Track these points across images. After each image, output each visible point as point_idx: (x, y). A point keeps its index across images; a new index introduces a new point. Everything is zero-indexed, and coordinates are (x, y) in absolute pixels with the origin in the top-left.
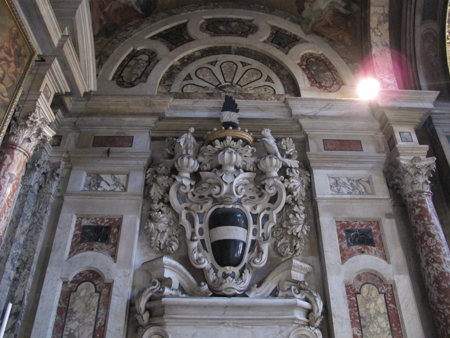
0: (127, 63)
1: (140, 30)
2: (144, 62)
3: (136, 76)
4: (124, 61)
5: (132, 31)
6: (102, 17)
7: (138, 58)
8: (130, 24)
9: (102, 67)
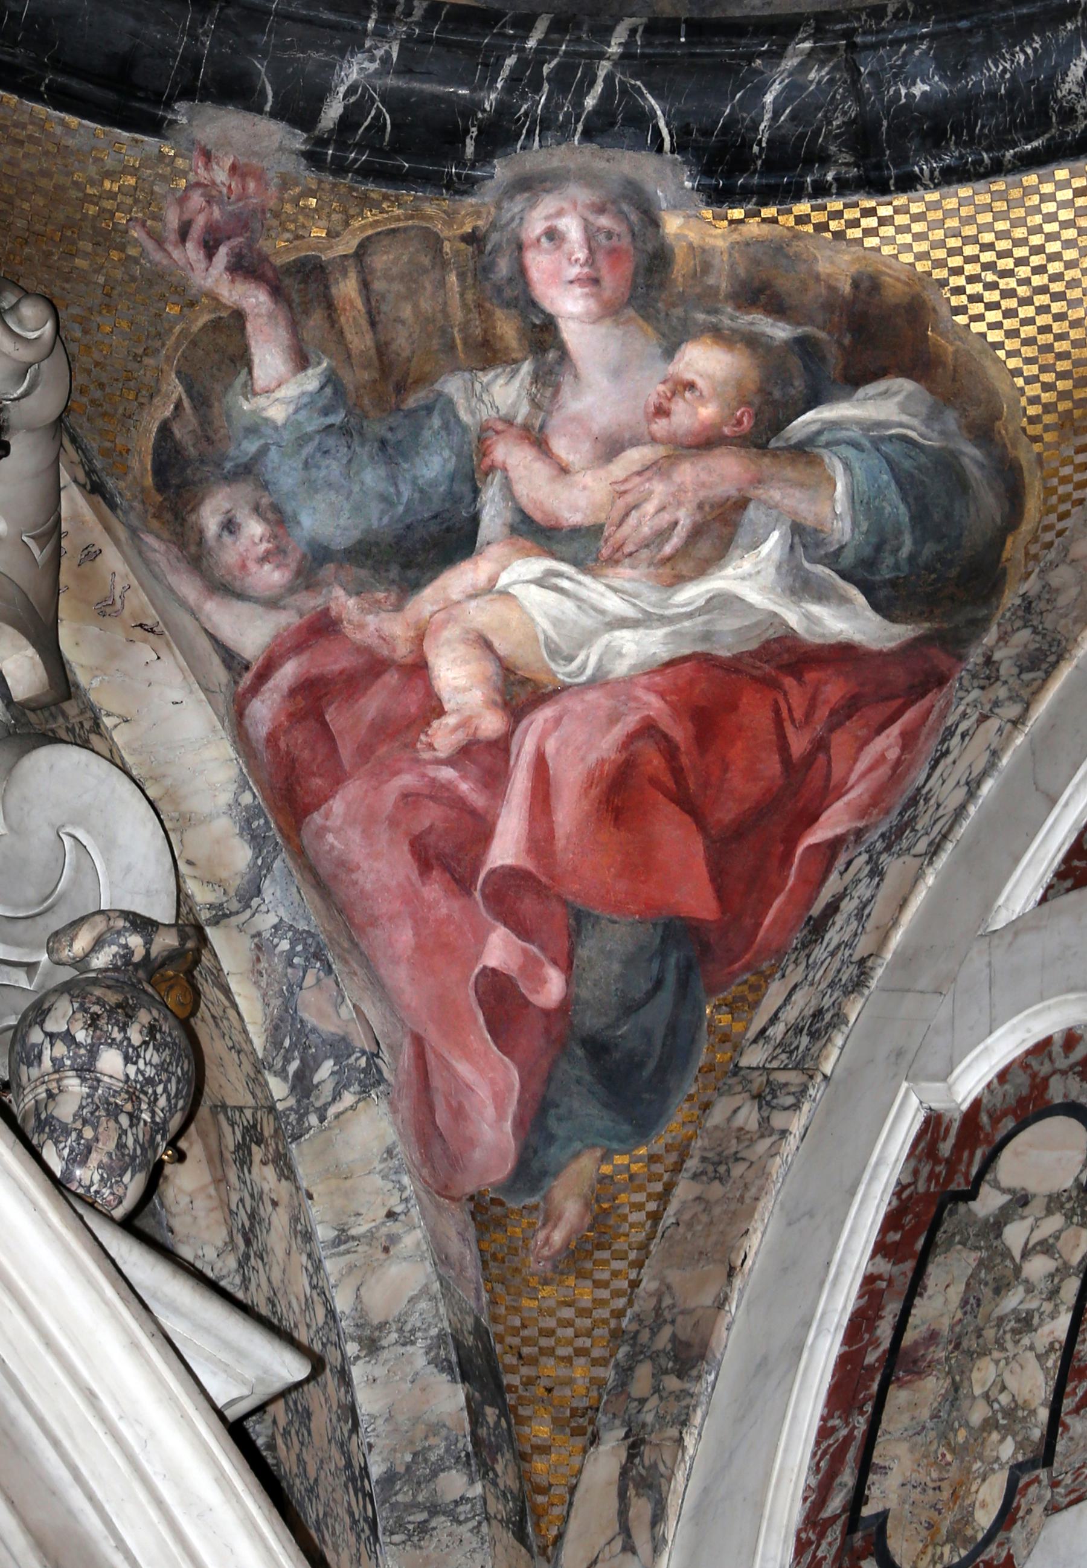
0: (900, 1328)
1: (935, 849)
2: (1056, 1222)
3: (1007, 1450)
4: (860, 1325)
5: (860, 914)
6: (499, 950)
7: (988, 1202)
8: (819, 834)
9: (658, 1517)
